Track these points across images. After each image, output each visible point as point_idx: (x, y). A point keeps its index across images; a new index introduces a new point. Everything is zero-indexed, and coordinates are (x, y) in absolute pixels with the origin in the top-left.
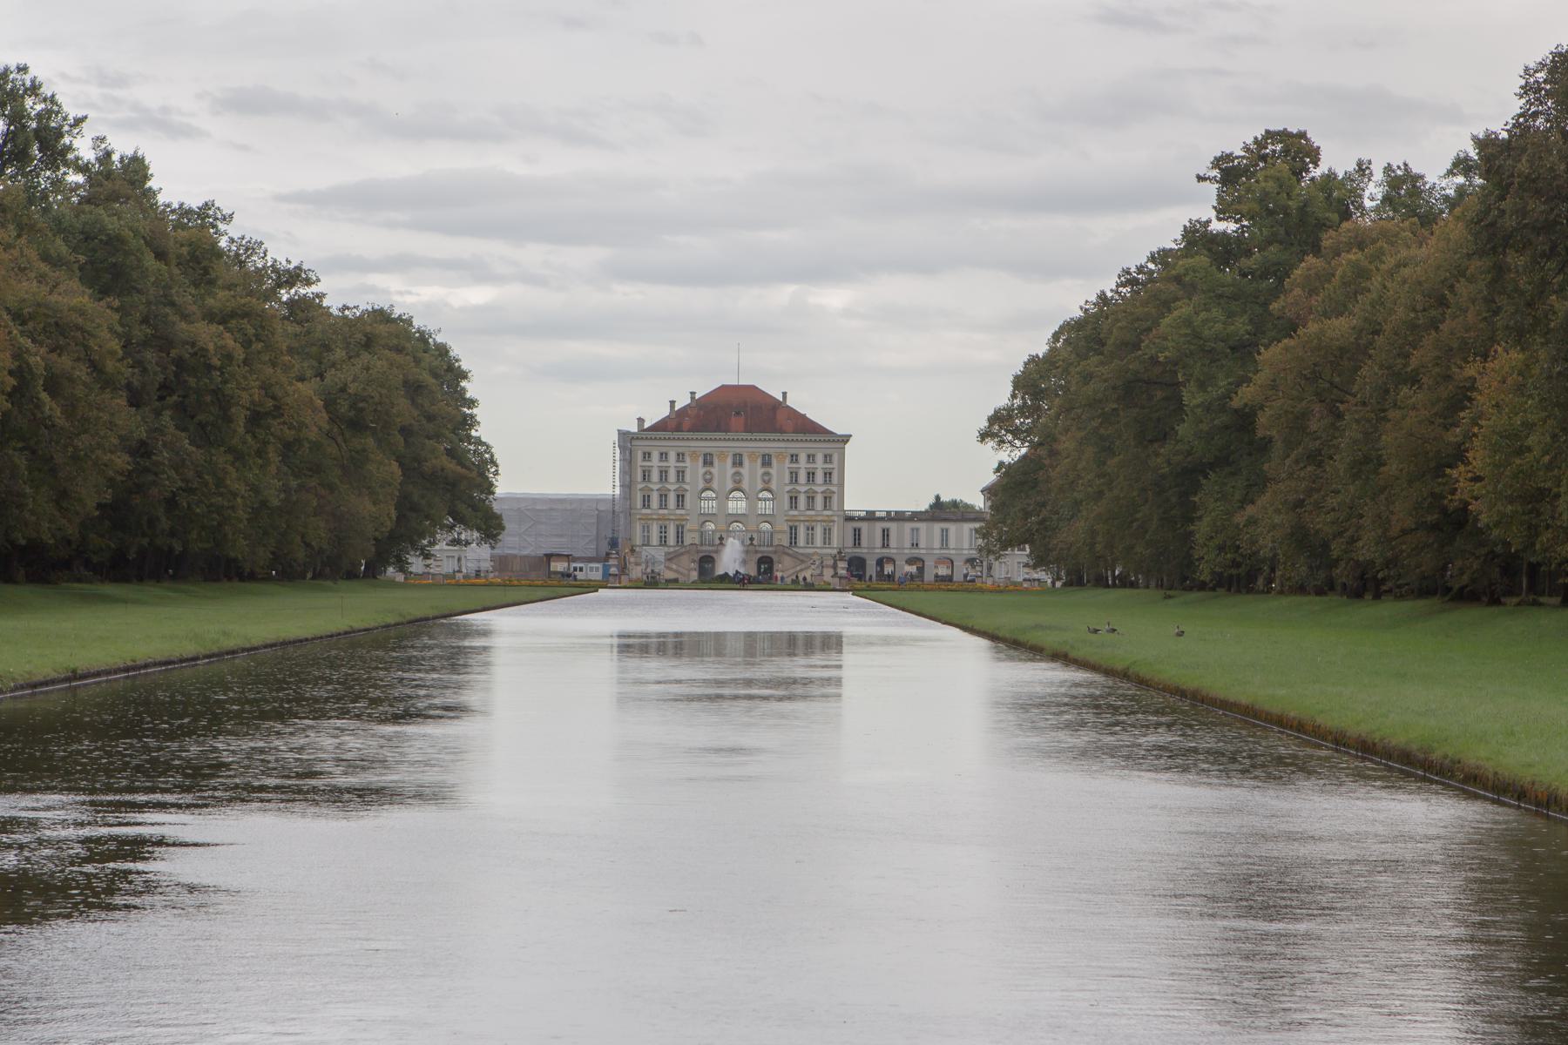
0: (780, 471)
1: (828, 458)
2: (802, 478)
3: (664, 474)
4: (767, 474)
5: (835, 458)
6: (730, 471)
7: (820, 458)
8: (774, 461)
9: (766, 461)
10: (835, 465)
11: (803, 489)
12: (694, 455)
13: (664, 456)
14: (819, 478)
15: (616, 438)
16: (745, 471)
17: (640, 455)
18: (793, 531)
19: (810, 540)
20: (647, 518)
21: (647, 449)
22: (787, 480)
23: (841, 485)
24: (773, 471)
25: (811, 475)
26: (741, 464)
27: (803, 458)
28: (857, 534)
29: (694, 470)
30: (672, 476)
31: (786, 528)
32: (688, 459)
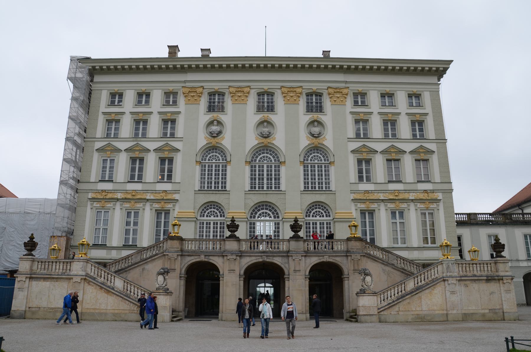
2: (376, 128)
3: (140, 122)
4: (320, 123)
5: (426, 97)
6: (253, 117)
7: (401, 98)
8: (327, 103)
10: (428, 108)
11: (380, 147)
12: (193, 94)
13: (143, 97)
14: (404, 128)
15: (64, 67)
17: (104, 97)
21: (116, 88)
22: (351, 133)
23: (442, 140)
24: (327, 118)
25: (390, 124)
26: (271, 109)
30: (154, 127)
31: (355, 214)
32: (181, 100)
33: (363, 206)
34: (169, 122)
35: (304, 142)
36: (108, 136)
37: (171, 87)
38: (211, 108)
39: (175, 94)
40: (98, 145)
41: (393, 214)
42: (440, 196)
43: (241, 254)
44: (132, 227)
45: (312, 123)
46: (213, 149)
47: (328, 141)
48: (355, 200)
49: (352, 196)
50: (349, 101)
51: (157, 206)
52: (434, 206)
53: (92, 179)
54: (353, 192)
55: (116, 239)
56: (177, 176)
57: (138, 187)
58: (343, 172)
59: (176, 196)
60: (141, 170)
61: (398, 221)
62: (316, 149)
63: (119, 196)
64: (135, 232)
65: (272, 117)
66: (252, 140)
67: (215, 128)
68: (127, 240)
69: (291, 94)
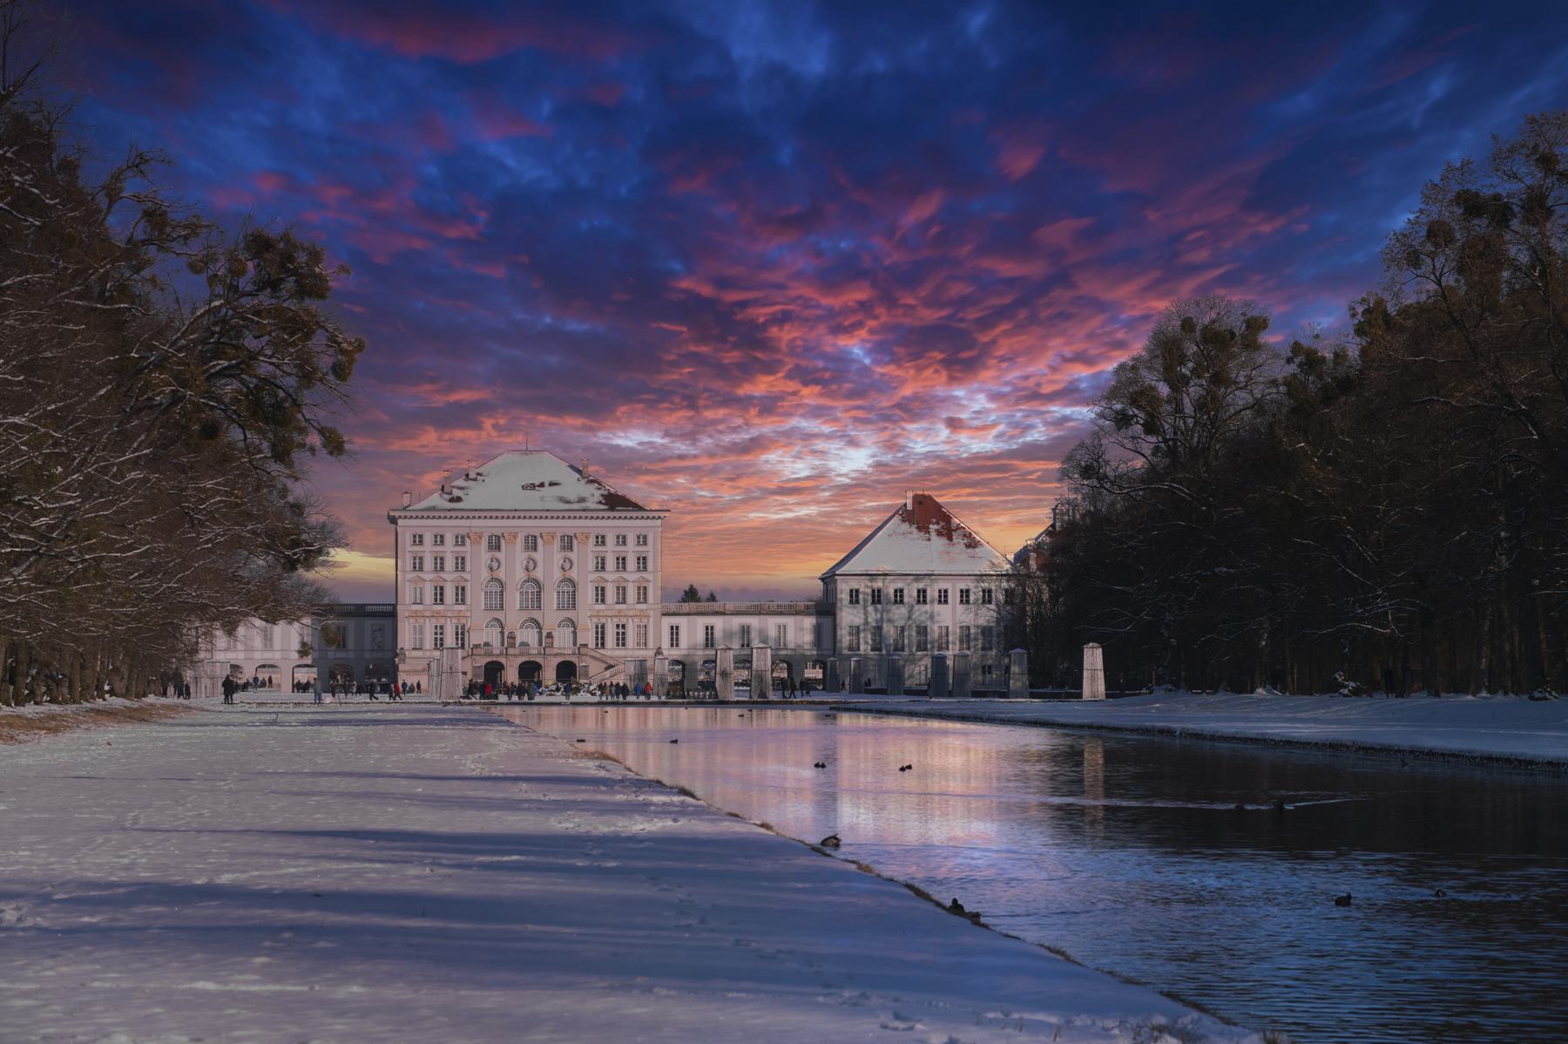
0: (585, 555)
2: (611, 564)
9: (567, 543)
10: (649, 547)
14: (631, 564)
16: (538, 556)
17: (409, 539)
19: (621, 640)
20: (416, 615)
24: (573, 556)
25: (622, 562)
27: (611, 540)
28: (675, 630)
29: (479, 557)
30: (450, 564)
32: (468, 541)
37: (463, 532)
47: (574, 574)
52: (645, 621)
55: (429, 643)
56: (468, 601)
65: (534, 555)
66: (521, 575)
67: (495, 565)
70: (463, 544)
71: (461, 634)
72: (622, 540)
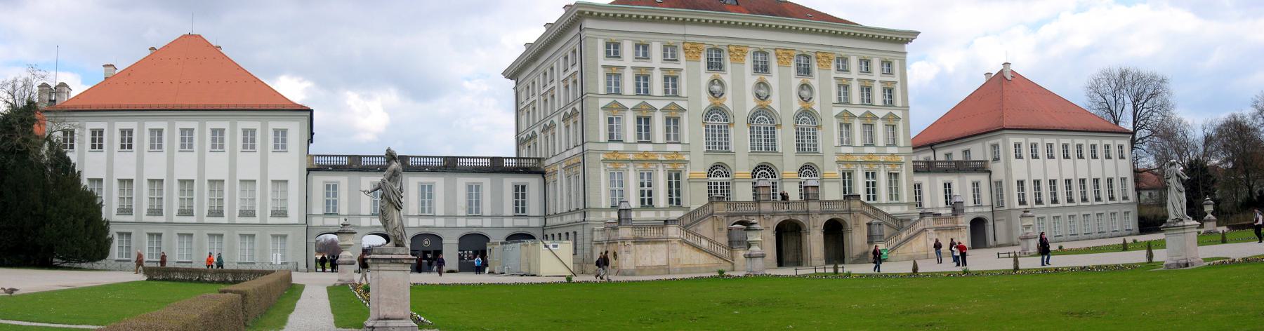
1: (888, 66)
3: (643, 79)
4: (809, 87)
5: (896, 65)
6: (751, 79)
11: (858, 112)
12: (693, 50)
13: (643, 49)
16: (773, 80)
18: (847, 177)
22: (835, 100)
23: (906, 108)
24: (814, 82)
29: (695, 79)
30: (657, 86)
32: (682, 56)
33: (844, 167)
34: (671, 80)
35: (797, 106)
36: (609, 93)
37: (671, 40)
38: (710, 66)
39: (674, 47)
40: (603, 102)
41: (867, 174)
42: (903, 159)
43: (774, 214)
44: (646, 189)
45: (802, 86)
46: (717, 110)
47: (816, 106)
48: (838, 162)
49: (836, 158)
50: (833, 66)
51: (669, 167)
53: (602, 140)
54: (838, 154)
55: (634, 201)
57: (649, 147)
58: (829, 137)
59: (686, 157)
60: (647, 129)
61: (871, 180)
62: (807, 113)
63: (631, 157)
64: (650, 193)
66: (751, 104)
67: (717, 88)
68: (643, 201)
69: (784, 55)
70: (674, 59)
71: (674, 182)
72: (866, 64)
